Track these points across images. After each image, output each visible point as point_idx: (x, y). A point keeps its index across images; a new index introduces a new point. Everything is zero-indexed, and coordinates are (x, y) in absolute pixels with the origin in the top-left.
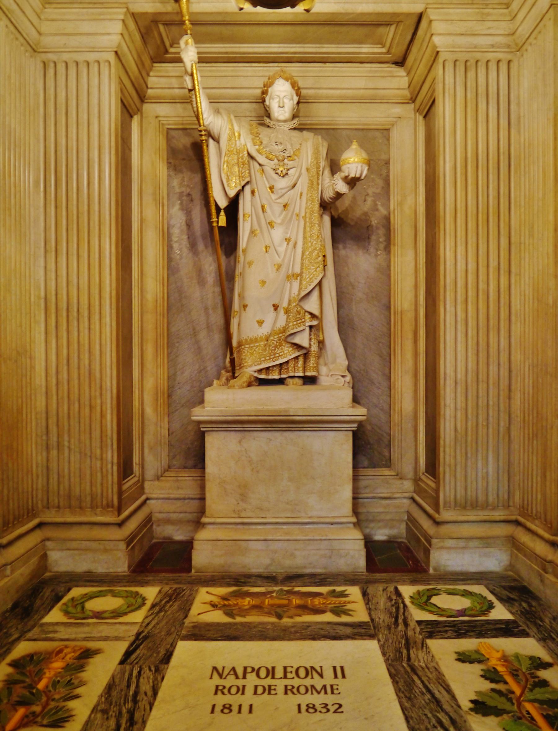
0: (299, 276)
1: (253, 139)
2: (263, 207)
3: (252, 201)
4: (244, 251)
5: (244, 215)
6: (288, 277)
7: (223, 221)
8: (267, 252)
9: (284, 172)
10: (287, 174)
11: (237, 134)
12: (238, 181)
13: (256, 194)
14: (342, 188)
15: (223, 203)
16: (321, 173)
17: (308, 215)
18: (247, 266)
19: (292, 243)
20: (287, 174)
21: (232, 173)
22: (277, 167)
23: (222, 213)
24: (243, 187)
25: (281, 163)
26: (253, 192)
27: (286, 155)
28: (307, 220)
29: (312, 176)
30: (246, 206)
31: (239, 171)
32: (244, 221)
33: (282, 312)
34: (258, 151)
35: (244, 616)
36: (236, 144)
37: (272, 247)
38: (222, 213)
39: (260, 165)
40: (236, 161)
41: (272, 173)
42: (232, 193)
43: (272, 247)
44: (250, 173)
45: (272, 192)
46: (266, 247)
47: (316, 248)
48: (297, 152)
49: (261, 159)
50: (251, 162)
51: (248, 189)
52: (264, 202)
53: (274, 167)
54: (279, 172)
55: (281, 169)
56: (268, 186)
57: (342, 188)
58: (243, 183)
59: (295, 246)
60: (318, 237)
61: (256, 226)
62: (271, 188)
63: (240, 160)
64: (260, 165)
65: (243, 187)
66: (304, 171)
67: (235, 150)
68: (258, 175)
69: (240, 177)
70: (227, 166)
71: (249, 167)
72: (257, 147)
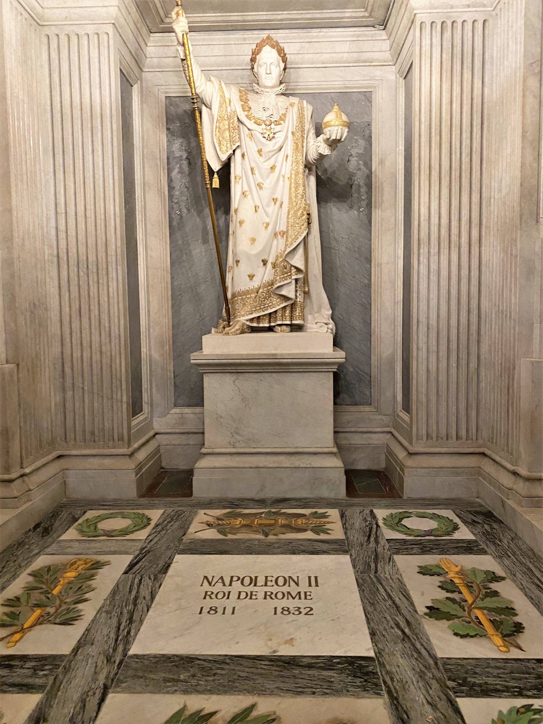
0: (284, 234)
1: (242, 105)
2: (252, 169)
3: (242, 164)
4: (236, 211)
5: (235, 177)
6: (275, 234)
7: (216, 183)
8: (256, 211)
9: (271, 135)
10: (273, 137)
11: (227, 101)
12: (229, 145)
13: (246, 157)
14: (325, 150)
15: (216, 167)
16: (305, 136)
17: (293, 176)
18: (238, 225)
19: (278, 203)
20: (273, 137)
21: (223, 138)
22: (265, 131)
23: (216, 176)
24: (234, 151)
25: (268, 128)
26: (243, 156)
27: (273, 120)
28: (293, 181)
29: (297, 139)
30: (236, 170)
31: (230, 136)
32: (235, 182)
33: (269, 265)
34: (247, 116)
35: (235, 534)
36: (227, 110)
37: (261, 207)
38: (216, 176)
39: (249, 129)
40: (227, 127)
41: (260, 137)
42: (224, 158)
43: (261, 207)
44: (240, 138)
45: (261, 155)
46: (255, 207)
47: (300, 207)
48: (283, 118)
49: (250, 124)
50: (241, 126)
51: (238, 153)
52: (253, 165)
53: (262, 131)
54: (266, 136)
55: (268, 133)
56: (256, 149)
57: (325, 150)
58: (234, 148)
59: (281, 206)
60: (302, 196)
61: (246, 188)
62: (260, 151)
63: (231, 125)
64: (249, 129)
65: (234, 151)
66: (290, 134)
67: (226, 116)
68: (248, 139)
69: (232, 141)
70: (219, 131)
71: (239, 131)
72: (246, 113)
